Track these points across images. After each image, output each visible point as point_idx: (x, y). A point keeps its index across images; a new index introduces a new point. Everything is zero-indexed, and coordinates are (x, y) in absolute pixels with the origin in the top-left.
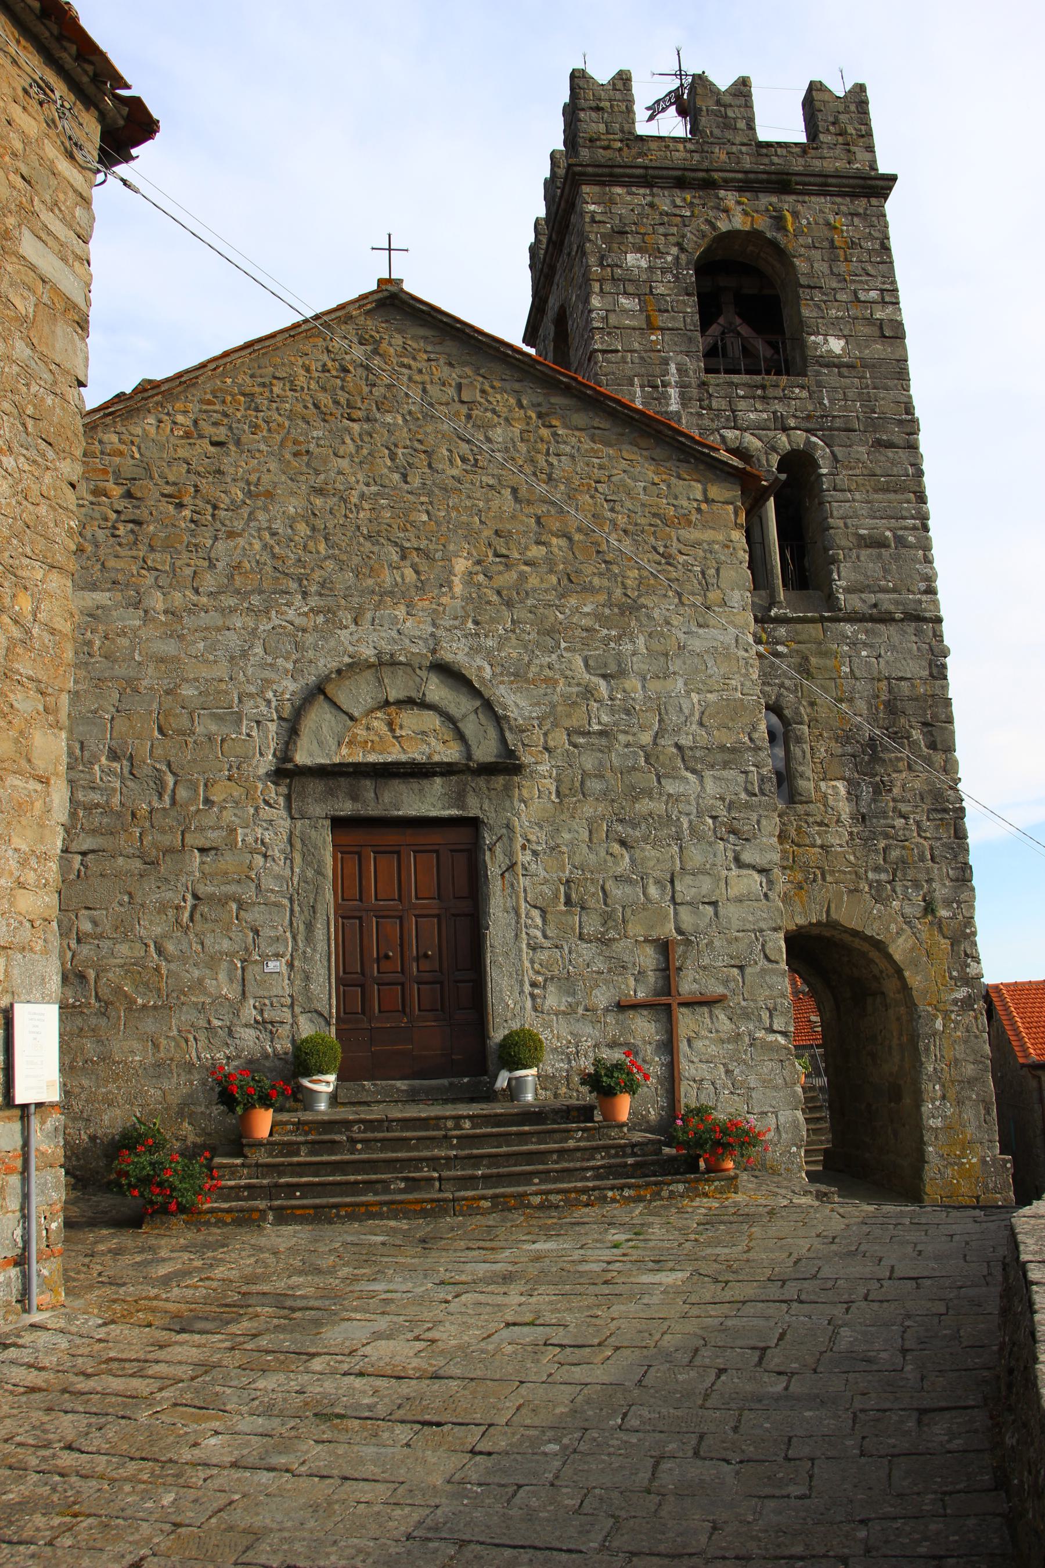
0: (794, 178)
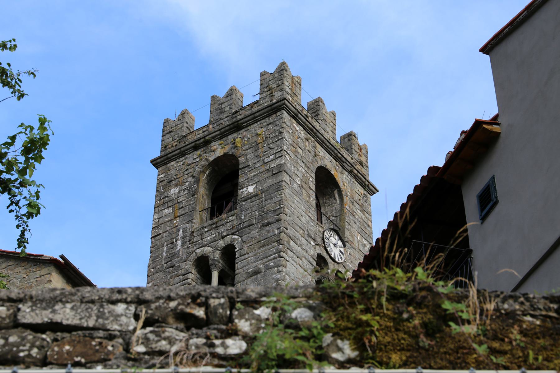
0: (242, 121)
